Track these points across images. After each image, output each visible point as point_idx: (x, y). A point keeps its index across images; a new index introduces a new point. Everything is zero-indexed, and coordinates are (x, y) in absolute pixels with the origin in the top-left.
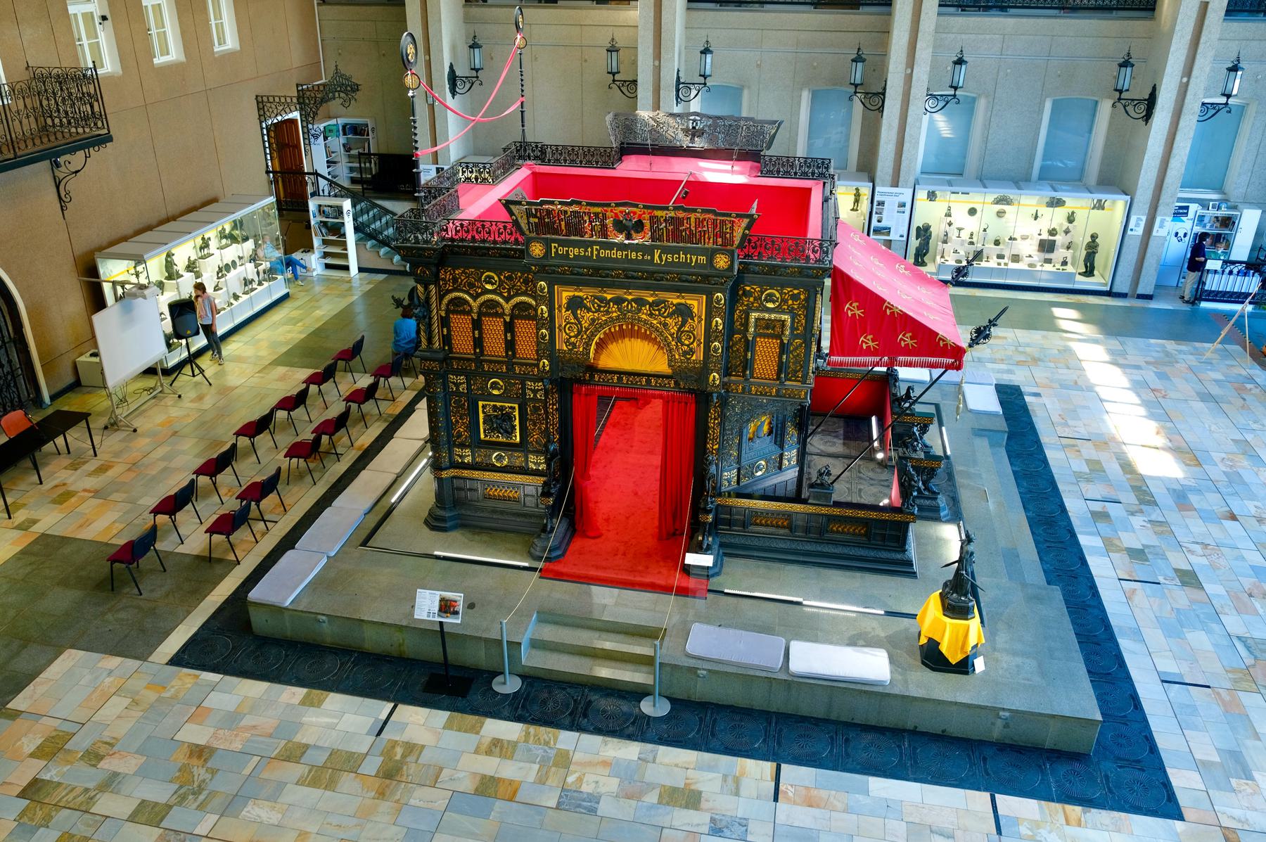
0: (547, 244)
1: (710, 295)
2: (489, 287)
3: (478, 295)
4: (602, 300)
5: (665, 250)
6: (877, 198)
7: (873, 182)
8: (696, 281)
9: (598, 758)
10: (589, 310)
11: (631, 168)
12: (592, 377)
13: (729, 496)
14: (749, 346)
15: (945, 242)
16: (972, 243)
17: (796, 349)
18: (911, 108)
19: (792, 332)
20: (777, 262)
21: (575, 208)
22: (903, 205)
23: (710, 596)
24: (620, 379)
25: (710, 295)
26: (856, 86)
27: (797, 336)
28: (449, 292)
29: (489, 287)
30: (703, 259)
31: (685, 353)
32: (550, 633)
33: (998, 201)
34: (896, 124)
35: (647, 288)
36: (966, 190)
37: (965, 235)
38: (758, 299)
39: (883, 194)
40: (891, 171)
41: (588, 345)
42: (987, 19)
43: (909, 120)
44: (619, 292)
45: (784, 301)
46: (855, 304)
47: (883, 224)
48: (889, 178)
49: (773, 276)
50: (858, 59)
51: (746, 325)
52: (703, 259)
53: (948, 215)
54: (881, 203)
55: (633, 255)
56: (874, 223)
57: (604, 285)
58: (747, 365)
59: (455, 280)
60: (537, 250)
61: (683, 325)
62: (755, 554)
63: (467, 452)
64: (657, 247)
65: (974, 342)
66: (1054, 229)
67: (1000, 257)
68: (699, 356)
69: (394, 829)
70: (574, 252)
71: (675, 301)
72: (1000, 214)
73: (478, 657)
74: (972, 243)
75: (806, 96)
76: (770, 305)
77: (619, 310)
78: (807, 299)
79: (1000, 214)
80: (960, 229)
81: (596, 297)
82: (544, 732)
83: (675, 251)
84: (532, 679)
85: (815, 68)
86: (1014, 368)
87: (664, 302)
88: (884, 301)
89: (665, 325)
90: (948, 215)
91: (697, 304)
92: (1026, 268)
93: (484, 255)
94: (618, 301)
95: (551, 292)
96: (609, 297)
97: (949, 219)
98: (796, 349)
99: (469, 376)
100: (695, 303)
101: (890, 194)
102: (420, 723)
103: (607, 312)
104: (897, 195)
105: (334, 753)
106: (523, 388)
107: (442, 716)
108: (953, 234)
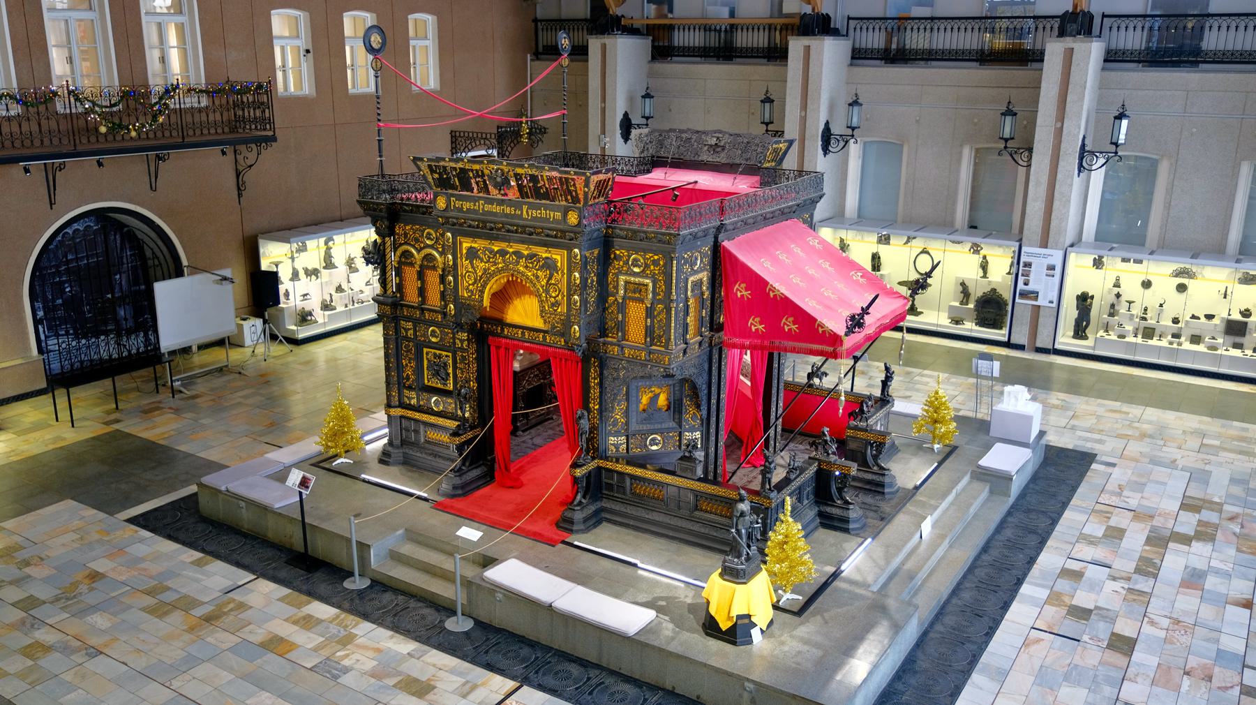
0: (449, 197)
1: (570, 250)
2: (428, 242)
3: (422, 249)
4: (491, 251)
5: (531, 206)
6: (1023, 259)
7: (1020, 240)
8: (556, 237)
9: (375, 645)
10: (482, 261)
11: (657, 177)
12: (502, 330)
13: (617, 461)
14: (622, 308)
15: (1111, 315)
16: (1144, 319)
17: (659, 314)
18: (1061, 163)
19: (654, 297)
20: (635, 227)
21: (460, 165)
22: (1052, 268)
23: (561, 546)
24: (523, 333)
25: (570, 250)
26: (1006, 140)
27: (660, 302)
28: (401, 245)
29: (428, 242)
30: (558, 215)
31: (553, 305)
32: (408, 549)
33: (1178, 274)
34: (1044, 179)
35: (523, 242)
36: (1139, 256)
37: (1136, 310)
38: (626, 263)
39: (1029, 254)
40: (1039, 231)
41: (482, 292)
42: (1158, 74)
43: (1059, 176)
44: (503, 245)
45: (647, 266)
46: (744, 285)
47: (1030, 287)
48: (1037, 238)
49: (638, 240)
50: (1009, 112)
51: (616, 287)
52: (558, 215)
53: (1117, 285)
54: (1028, 265)
55: (508, 210)
56: (1020, 286)
57: (492, 238)
58: (621, 327)
59: (406, 235)
60: (441, 203)
61: (550, 279)
62: (632, 522)
63: (413, 394)
64: (525, 203)
65: (850, 331)
66: (1247, 310)
67: (1176, 336)
68: (562, 309)
69: (180, 652)
70: (467, 205)
71: (544, 255)
72: (1182, 288)
73: (337, 555)
74: (1144, 319)
75: (967, 154)
76: (636, 270)
77: (504, 261)
78: (665, 265)
79: (1182, 288)
80: (1130, 303)
81: (487, 249)
82: (351, 619)
83: (538, 207)
84: (380, 585)
85: (975, 124)
86: (1104, 438)
87: (535, 255)
88: (767, 283)
89: (537, 277)
90: (1117, 285)
91: (559, 256)
92: (1205, 350)
93: (424, 213)
94: (503, 253)
95: (454, 243)
96: (496, 249)
97: (1116, 290)
98: (659, 314)
99: (416, 322)
100: (558, 257)
101: (1037, 256)
102: (265, 593)
103: (495, 264)
104: (1045, 256)
105: (186, 596)
106: (454, 338)
107: (285, 591)
108: (1123, 310)
